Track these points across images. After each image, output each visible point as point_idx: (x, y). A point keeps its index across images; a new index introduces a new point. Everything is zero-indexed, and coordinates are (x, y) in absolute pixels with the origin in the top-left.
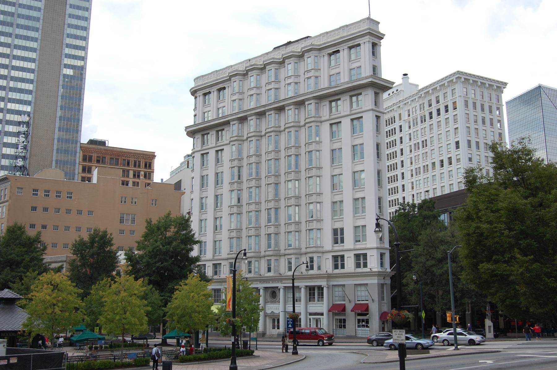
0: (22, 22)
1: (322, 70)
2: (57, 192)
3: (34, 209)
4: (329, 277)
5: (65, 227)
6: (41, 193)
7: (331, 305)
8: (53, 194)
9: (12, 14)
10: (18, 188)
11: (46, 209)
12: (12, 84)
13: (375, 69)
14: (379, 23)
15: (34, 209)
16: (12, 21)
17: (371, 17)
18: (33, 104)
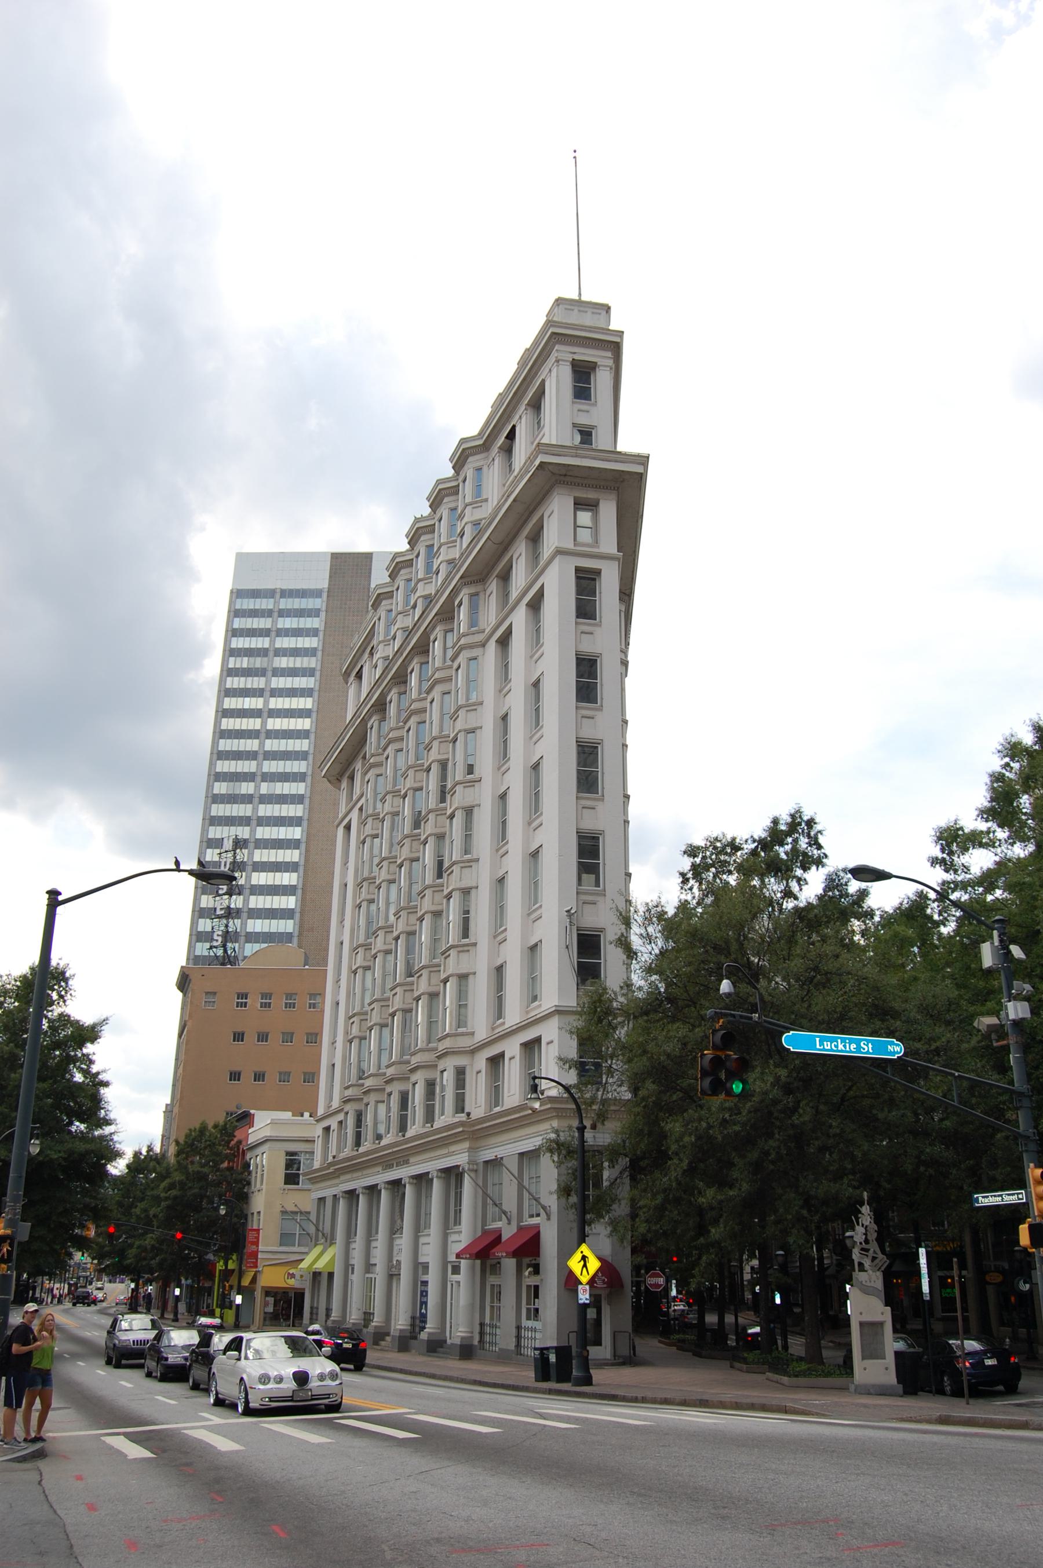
0: (283, 662)
2: (264, 996)
3: (239, 1037)
4: (475, 1133)
5: (305, 1074)
6: (254, 1002)
7: (479, 1233)
8: (278, 1002)
9: (263, 652)
10: (207, 993)
11: (263, 1037)
12: (265, 788)
13: (586, 434)
14: (607, 309)
15: (239, 1037)
16: (265, 665)
17: (583, 298)
18: (305, 823)
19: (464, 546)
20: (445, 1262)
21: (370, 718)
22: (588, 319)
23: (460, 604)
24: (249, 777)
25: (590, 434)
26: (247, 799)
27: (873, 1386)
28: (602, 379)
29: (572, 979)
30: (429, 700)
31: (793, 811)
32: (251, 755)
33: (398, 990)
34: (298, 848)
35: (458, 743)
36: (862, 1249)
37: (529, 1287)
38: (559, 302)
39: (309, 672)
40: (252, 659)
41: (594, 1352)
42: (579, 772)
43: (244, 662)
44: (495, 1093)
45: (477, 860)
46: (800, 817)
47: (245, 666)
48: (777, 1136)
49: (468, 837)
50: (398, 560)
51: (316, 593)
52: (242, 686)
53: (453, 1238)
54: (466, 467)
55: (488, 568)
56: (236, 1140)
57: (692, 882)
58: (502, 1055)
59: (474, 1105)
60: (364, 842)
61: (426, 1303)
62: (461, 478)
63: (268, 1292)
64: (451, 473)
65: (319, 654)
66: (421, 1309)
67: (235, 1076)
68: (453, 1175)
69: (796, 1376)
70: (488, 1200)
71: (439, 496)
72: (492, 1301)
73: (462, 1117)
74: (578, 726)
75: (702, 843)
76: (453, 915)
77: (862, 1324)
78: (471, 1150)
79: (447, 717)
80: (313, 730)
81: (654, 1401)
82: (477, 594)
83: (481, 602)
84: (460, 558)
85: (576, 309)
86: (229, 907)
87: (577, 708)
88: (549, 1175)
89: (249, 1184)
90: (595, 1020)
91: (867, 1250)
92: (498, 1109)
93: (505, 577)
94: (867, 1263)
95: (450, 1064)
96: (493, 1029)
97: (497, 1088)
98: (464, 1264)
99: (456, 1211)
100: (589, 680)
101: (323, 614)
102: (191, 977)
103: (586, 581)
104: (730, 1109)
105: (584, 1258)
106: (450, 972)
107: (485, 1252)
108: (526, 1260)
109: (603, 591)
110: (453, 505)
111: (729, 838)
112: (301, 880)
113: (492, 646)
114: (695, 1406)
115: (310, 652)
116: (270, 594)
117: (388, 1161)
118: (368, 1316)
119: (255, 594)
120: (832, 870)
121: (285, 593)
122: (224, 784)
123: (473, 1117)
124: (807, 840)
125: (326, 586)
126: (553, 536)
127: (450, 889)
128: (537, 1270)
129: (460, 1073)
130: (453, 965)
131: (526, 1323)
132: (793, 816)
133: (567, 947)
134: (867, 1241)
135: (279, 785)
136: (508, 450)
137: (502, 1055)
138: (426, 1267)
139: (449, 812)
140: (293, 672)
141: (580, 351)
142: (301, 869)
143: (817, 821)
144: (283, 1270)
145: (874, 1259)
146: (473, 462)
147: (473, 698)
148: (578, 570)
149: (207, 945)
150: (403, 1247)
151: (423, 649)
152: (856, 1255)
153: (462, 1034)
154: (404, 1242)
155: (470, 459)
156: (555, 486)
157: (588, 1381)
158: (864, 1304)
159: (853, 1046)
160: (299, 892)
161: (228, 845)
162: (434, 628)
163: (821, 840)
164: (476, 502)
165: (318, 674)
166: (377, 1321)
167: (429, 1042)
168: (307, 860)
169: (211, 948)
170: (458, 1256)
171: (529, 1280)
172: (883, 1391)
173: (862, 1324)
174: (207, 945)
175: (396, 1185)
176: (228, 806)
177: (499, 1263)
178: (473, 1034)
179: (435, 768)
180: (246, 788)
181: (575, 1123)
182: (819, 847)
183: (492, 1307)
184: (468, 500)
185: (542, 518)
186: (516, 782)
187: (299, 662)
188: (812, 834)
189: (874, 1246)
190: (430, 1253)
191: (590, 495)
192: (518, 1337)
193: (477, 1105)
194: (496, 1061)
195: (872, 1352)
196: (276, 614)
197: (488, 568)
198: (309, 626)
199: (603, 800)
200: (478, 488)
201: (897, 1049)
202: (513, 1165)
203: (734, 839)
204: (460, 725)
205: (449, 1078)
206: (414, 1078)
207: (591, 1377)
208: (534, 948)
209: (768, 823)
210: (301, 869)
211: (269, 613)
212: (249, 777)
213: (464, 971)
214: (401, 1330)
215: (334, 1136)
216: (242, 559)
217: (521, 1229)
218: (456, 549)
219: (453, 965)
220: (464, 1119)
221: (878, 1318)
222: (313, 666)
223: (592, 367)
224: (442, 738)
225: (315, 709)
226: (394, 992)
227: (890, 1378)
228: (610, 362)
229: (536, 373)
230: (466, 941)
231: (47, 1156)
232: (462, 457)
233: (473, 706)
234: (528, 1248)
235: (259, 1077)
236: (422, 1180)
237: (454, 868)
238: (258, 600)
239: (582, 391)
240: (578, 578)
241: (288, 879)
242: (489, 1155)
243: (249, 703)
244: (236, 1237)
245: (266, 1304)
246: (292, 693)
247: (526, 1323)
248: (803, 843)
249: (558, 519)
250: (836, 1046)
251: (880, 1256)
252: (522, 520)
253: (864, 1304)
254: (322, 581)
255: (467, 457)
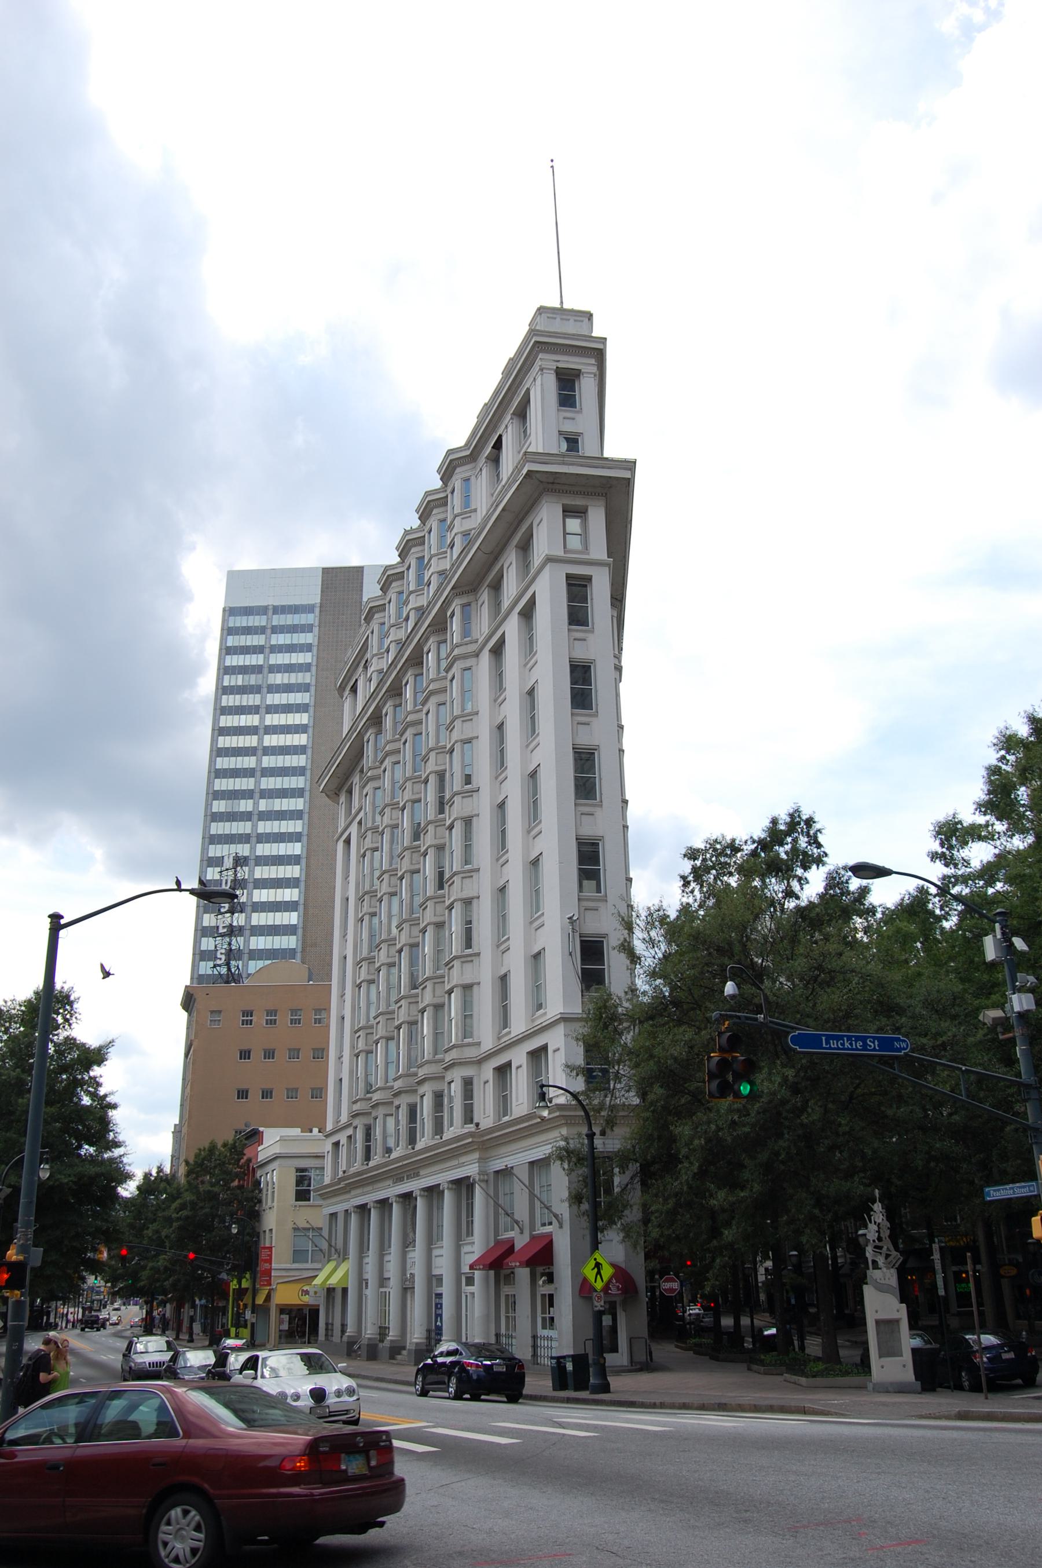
0: (278, 679)
1: (479, 510)
2: (269, 1013)
3: (245, 1054)
4: (485, 1143)
5: (313, 1089)
6: (259, 1019)
7: (492, 1244)
8: (284, 1019)
9: (257, 669)
10: (212, 1012)
11: (269, 1054)
12: (263, 805)
13: (573, 442)
14: (589, 316)
15: (245, 1054)
16: (260, 682)
17: (566, 306)
18: (305, 839)
19: (455, 557)
20: (458, 1274)
21: (366, 732)
22: (571, 327)
23: (453, 615)
24: (247, 794)
25: (576, 441)
26: (246, 816)
27: (892, 1384)
28: (586, 387)
29: (576, 986)
30: (424, 712)
31: (791, 811)
32: (248, 773)
33: (403, 1002)
34: (298, 864)
35: (455, 753)
36: (876, 1247)
37: (543, 1296)
38: (541, 310)
39: (304, 688)
40: (246, 677)
41: (611, 1359)
42: (576, 778)
43: (239, 680)
44: (503, 1102)
45: (478, 870)
46: (799, 816)
47: (240, 683)
48: (786, 1136)
49: (468, 848)
50: (389, 573)
51: (309, 609)
52: (237, 704)
53: (466, 1249)
54: (454, 478)
55: (479, 578)
56: (245, 1158)
57: (693, 885)
58: (509, 1064)
59: (483, 1116)
60: (364, 856)
61: (441, 1315)
62: (449, 489)
63: (283, 1310)
64: (439, 484)
65: (314, 669)
66: (436, 1321)
67: (243, 1094)
68: (463, 1186)
69: (814, 1376)
70: (499, 1209)
71: (430, 507)
72: (507, 1312)
73: (471, 1128)
74: (574, 734)
75: (702, 846)
76: (456, 926)
77: (878, 1322)
78: (481, 1160)
79: (442, 728)
80: (310, 745)
81: (672, 1406)
82: (469, 604)
83: (473, 613)
84: (451, 569)
85: (558, 317)
86: (231, 925)
87: (572, 714)
88: (560, 1183)
89: (260, 1201)
90: (601, 1027)
91: (880, 1248)
92: (506, 1119)
93: (497, 587)
94: (881, 1260)
95: (457, 1075)
96: (499, 1039)
97: (505, 1097)
98: (477, 1274)
99: (468, 1222)
100: (584, 686)
101: (316, 630)
102: (195, 996)
103: (578, 588)
104: (738, 1110)
105: (598, 1265)
106: (454, 983)
107: (498, 1262)
108: (540, 1269)
109: (595, 596)
110: (441, 516)
111: (728, 839)
112: (302, 895)
113: (485, 656)
114: (713, 1410)
115: (305, 668)
116: (263, 610)
117: (399, 1175)
118: (383, 1331)
119: (248, 611)
120: (832, 868)
121: (279, 610)
122: (223, 802)
123: (482, 1127)
124: (806, 839)
125: (319, 601)
126: (543, 544)
127: (452, 900)
128: (550, 1279)
129: (468, 1084)
130: (457, 976)
131: (542, 1332)
132: (791, 816)
133: (570, 954)
134: (880, 1239)
135: (277, 801)
136: (495, 460)
137: (509, 1064)
138: (439, 1279)
139: (448, 823)
140: (288, 688)
141: (563, 359)
142: (302, 884)
143: (816, 820)
144: (297, 1286)
145: (887, 1256)
146: (461, 473)
147: (469, 708)
148: (569, 577)
149: (211, 964)
150: (416, 1260)
151: (417, 660)
152: (869, 1252)
153: (469, 1045)
154: (417, 1255)
155: (458, 470)
156: (544, 492)
157: (606, 1388)
158: (881, 1302)
159: (859, 1044)
160: (301, 908)
161: (228, 863)
162: (427, 639)
163: (821, 838)
164: (466, 513)
165: (313, 689)
166: (393, 1335)
167: (436, 1053)
168: (307, 875)
169: (215, 966)
170: (471, 1267)
171: (544, 1289)
172: (901, 1389)
173: (878, 1322)
174: (211, 964)
175: (407, 1198)
176: (227, 824)
177: (513, 1273)
178: (479, 1044)
179: (432, 779)
180: (245, 805)
181: (585, 1130)
182: (819, 846)
183: (507, 1317)
184: (457, 511)
185: (531, 526)
186: (514, 790)
187: (294, 678)
188: (812, 832)
189: (887, 1244)
190: (443, 1265)
191: (578, 502)
192: (535, 1347)
193: (486, 1115)
194: (503, 1071)
195: (889, 1350)
196: (269, 631)
197: (479, 578)
198: (302, 641)
199: (601, 806)
200: (467, 499)
201: (903, 1045)
202: (523, 1174)
203: (733, 840)
204: (456, 735)
205: (456, 1089)
206: (421, 1090)
207: (609, 1384)
208: (537, 956)
209: (767, 823)
210: (302, 884)
211: (261, 630)
212: (247, 794)
213: (469, 981)
214: (417, 1344)
215: (343, 1151)
216: (235, 579)
217: (533, 1238)
218: (446, 560)
219: (457, 976)
220: (473, 1130)
221: (895, 1315)
222: (308, 681)
223: (577, 374)
224: (439, 749)
225: (311, 724)
226: (399, 1005)
227: (908, 1375)
228: (594, 369)
229: (521, 383)
230: (469, 951)
231: (58, 1180)
232: (450, 467)
233: (469, 717)
234: (542, 1257)
235: (267, 1094)
236: (433, 1192)
237: (455, 878)
238: (251, 618)
239: (567, 398)
240: (569, 585)
241: (289, 895)
242: (499, 1165)
243: (244, 720)
244: (249, 1255)
245: (281, 1322)
246: (287, 709)
247: (542, 1332)
248: (803, 842)
249: (548, 528)
250: (843, 1044)
251: (894, 1253)
252: (512, 529)
253: (881, 1302)
254: (315, 598)
255: (455, 468)
